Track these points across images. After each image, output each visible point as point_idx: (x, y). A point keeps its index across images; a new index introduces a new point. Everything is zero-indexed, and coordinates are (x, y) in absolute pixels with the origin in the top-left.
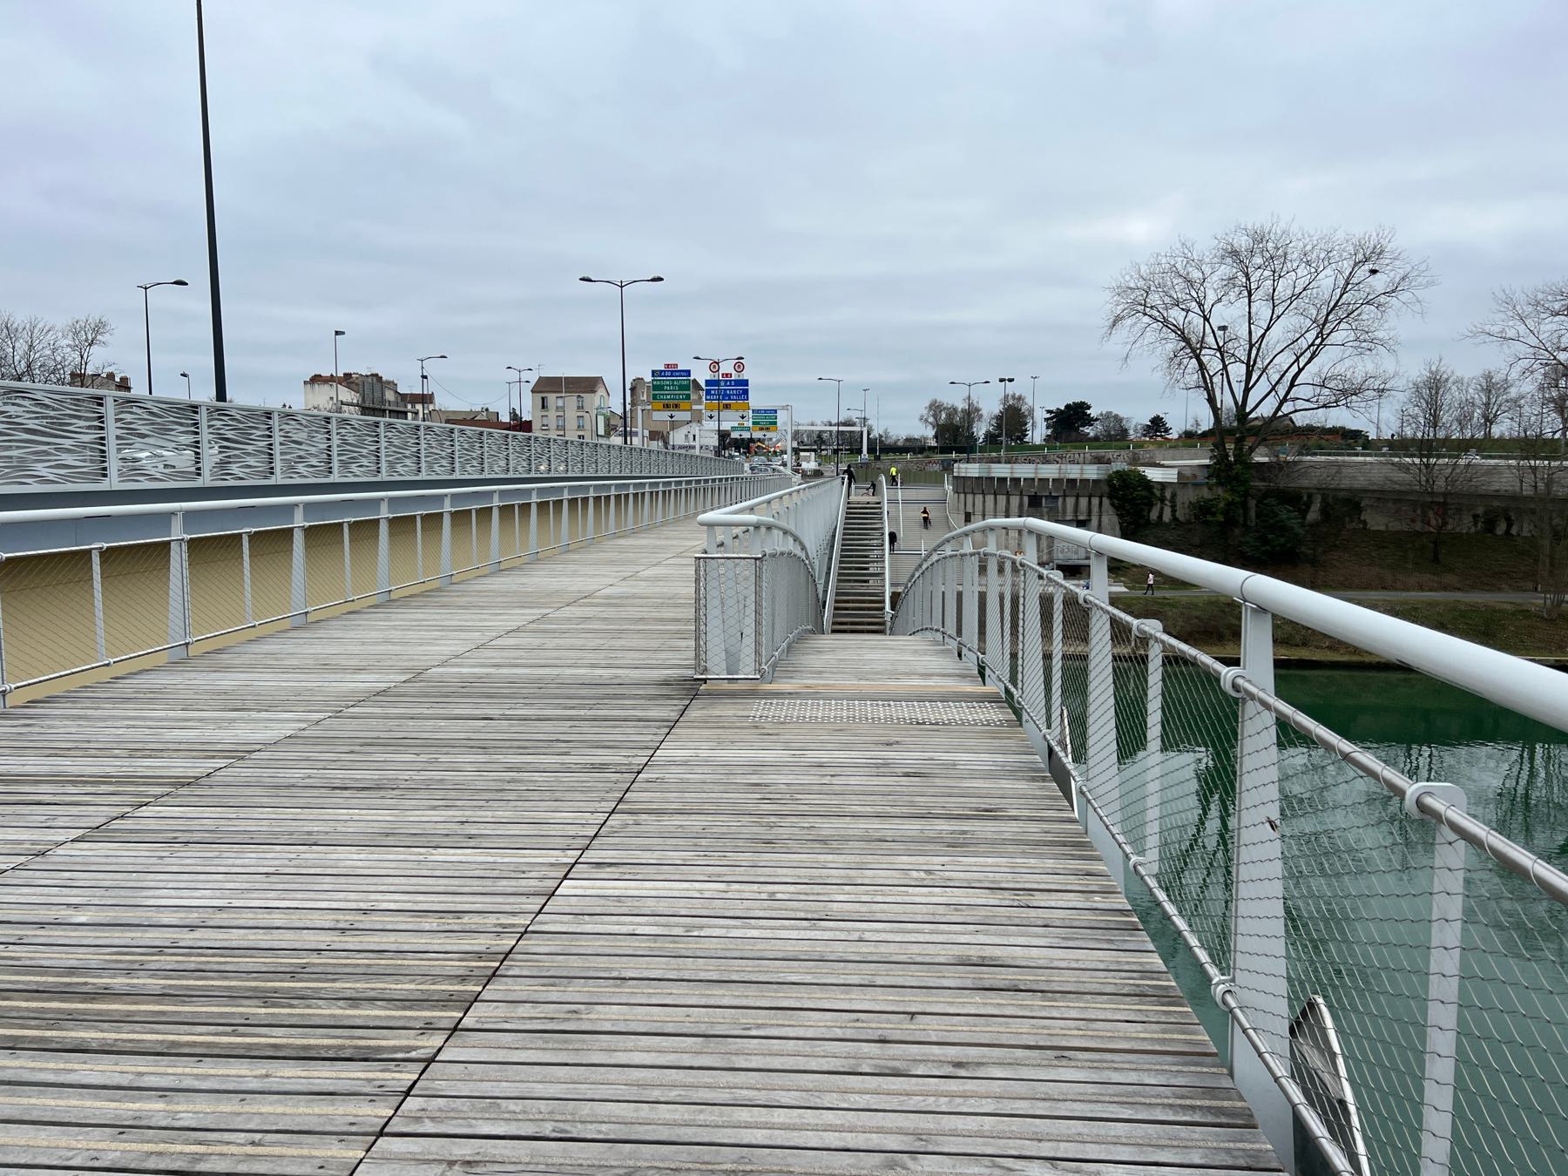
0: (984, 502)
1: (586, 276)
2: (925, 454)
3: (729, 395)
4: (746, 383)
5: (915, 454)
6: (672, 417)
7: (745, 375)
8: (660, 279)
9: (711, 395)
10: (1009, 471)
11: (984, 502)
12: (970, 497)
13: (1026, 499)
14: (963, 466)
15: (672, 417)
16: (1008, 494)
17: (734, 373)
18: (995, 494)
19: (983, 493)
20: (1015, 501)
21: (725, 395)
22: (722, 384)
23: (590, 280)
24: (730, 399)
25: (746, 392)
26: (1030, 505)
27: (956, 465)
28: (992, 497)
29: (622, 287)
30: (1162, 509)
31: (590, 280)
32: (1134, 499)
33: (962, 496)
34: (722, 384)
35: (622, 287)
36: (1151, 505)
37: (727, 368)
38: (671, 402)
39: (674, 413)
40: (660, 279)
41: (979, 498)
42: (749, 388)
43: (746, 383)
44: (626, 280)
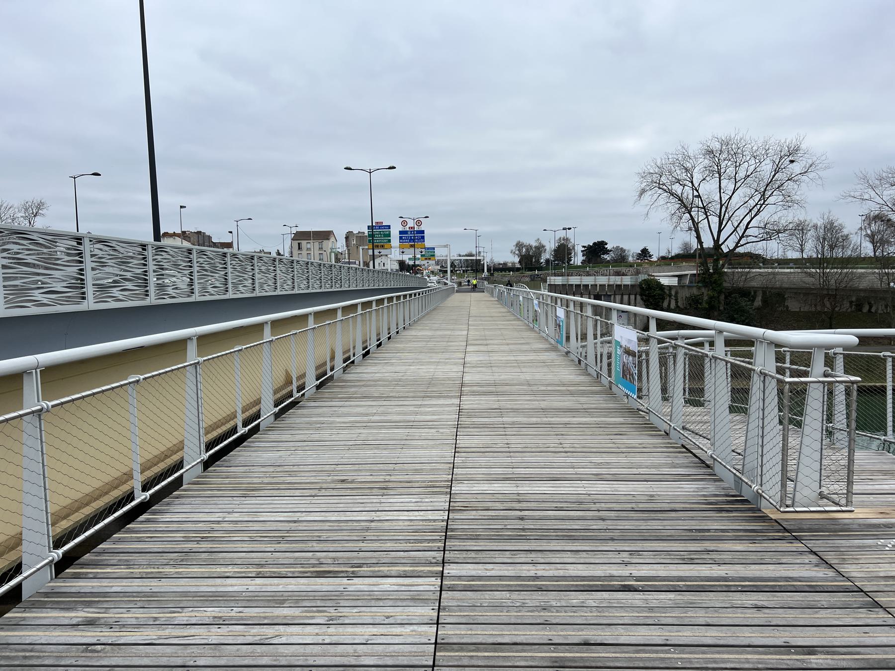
1: (348, 166)
2: (520, 272)
4: (423, 232)
6: (380, 253)
7: (422, 228)
8: (394, 168)
10: (580, 280)
14: (552, 278)
15: (380, 253)
17: (416, 226)
21: (411, 239)
22: (409, 233)
23: (351, 169)
25: (423, 237)
27: (548, 278)
29: (370, 173)
30: (670, 301)
31: (351, 169)
32: (655, 295)
34: (409, 233)
35: (370, 173)
36: (663, 299)
37: (411, 224)
38: (379, 244)
39: (381, 251)
40: (394, 168)
42: (425, 235)
43: (423, 232)
44: (373, 168)
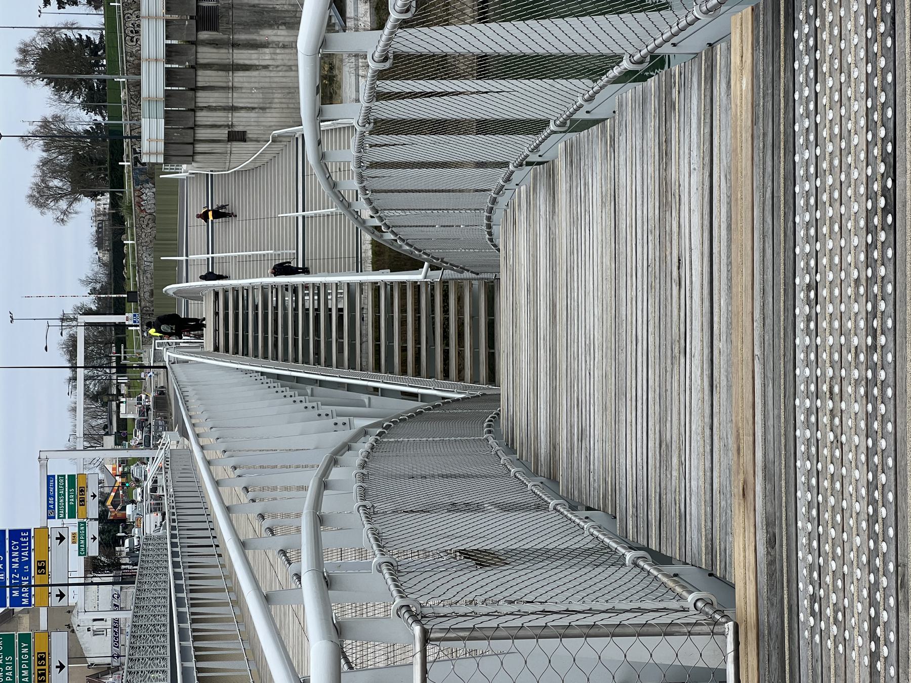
0: (209, 108)
2: (124, 212)
3: (22, 564)
5: (123, 231)
6: (61, 667)
9: (20, 597)
10: (153, 56)
11: (209, 108)
12: (202, 134)
13: (204, 35)
14: (145, 146)
16: (195, 67)
18: (195, 89)
19: (193, 110)
20: (206, 54)
21: (21, 571)
24: (29, 563)
26: (215, 28)
27: (145, 159)
28: (200, 94)
33: (200, 147)
38: (35, 668)
39: (55, 663)
41: (203, 117)
